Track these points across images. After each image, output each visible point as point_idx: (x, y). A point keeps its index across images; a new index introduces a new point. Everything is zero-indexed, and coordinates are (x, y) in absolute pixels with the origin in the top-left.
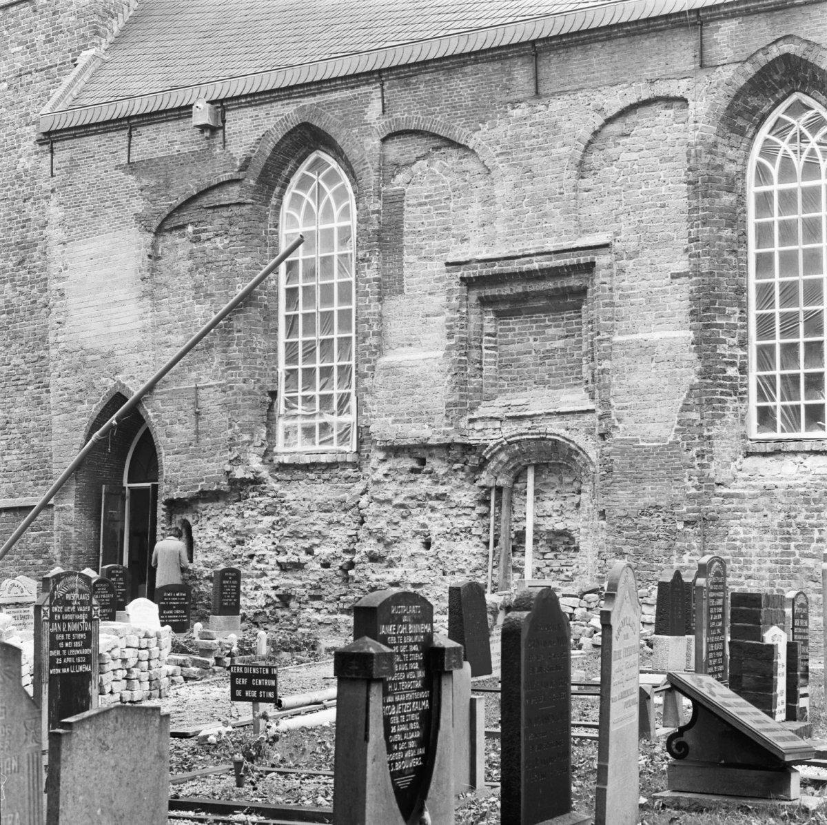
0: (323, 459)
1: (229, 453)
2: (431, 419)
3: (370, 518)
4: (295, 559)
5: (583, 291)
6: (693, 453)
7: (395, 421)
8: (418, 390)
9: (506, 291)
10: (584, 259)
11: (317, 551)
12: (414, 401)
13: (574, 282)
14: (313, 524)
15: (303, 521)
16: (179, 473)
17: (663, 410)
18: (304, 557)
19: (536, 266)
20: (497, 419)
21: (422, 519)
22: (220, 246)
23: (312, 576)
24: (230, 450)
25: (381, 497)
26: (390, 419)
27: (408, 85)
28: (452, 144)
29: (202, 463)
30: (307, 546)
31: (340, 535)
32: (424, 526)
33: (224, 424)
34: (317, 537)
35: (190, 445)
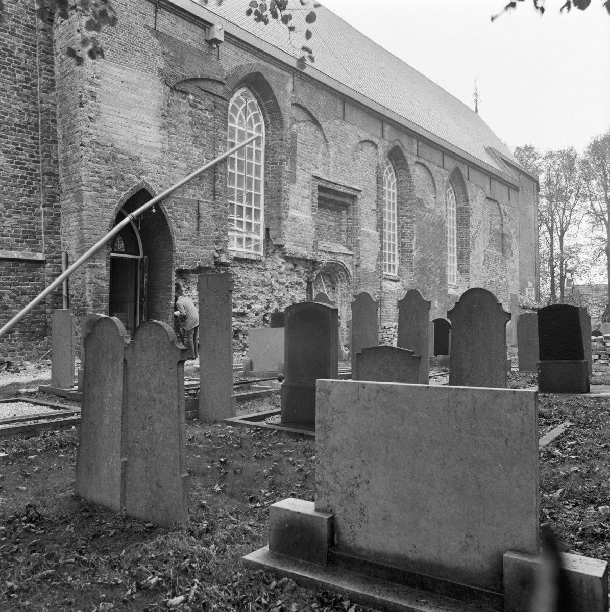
0: (252, 257)
1: (216, 246)
2: (307, 247)
3: (277, 291)
4: (242, 311)
5: (346, 206)
6: (378, 276)
7: (294, 245)
8: (303, 232)
9: (340, 199)
10: (355, 193)
11: (253, 307)
12: (302, 237)
13: (347, 201)
14: (253, 292)
15: (248, 290)
16: (185, 253)
17: (372, 259)
18: (247, 310)
19: (342, 190)
20: (325, 252)
21: (292, 293)
22: (209, 117)
23: (250, 320)
24: (216, 244)
25: (280, 280)
26: (292, 243)
27: (303, 84)
28: (316, 122)
29: (198, 249)
30: (248, 303)
31: (263, 298)
32: (293, 296)
33: (213, 228)
34: (254, 299)
35: (193, 236)
